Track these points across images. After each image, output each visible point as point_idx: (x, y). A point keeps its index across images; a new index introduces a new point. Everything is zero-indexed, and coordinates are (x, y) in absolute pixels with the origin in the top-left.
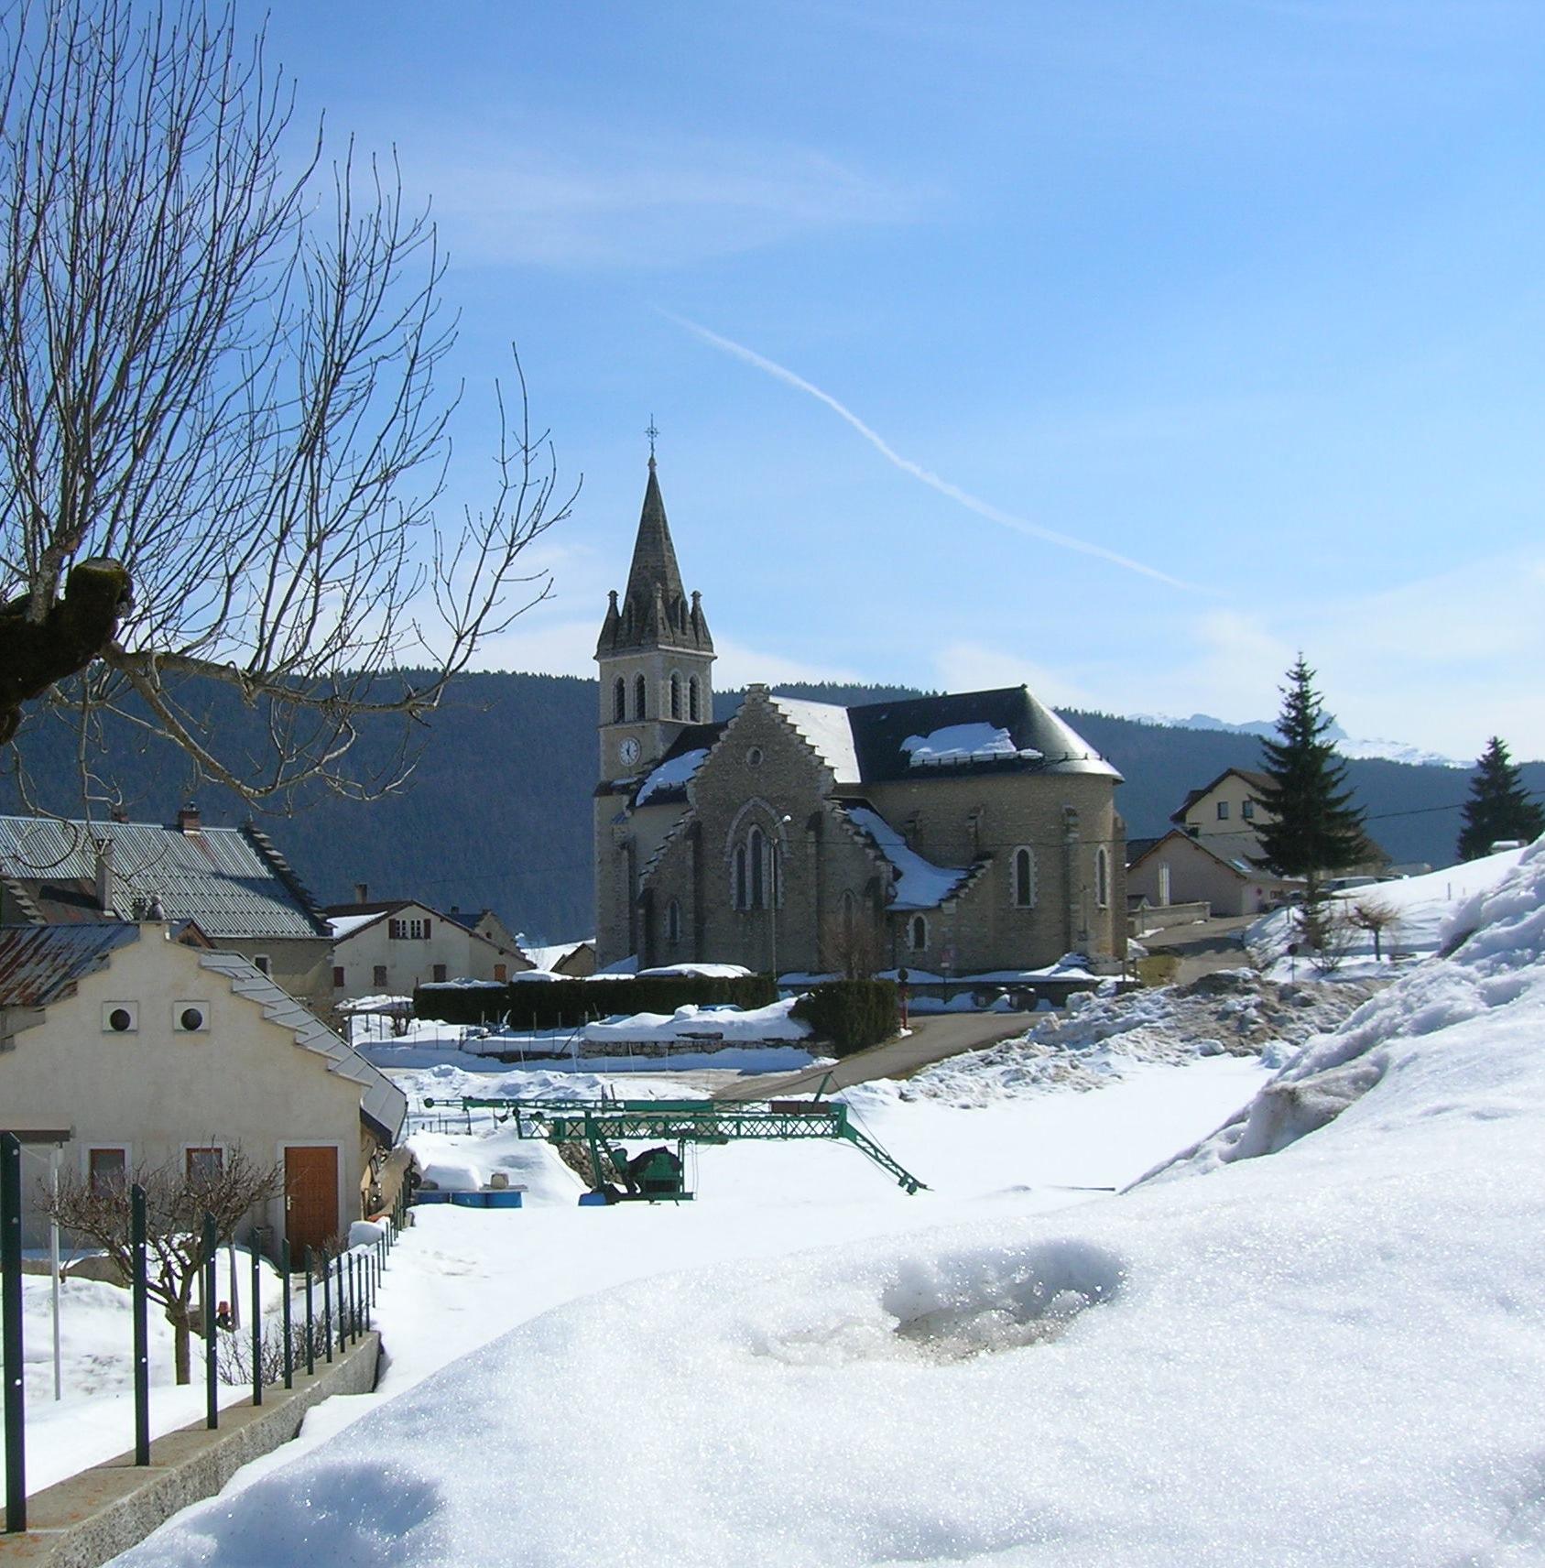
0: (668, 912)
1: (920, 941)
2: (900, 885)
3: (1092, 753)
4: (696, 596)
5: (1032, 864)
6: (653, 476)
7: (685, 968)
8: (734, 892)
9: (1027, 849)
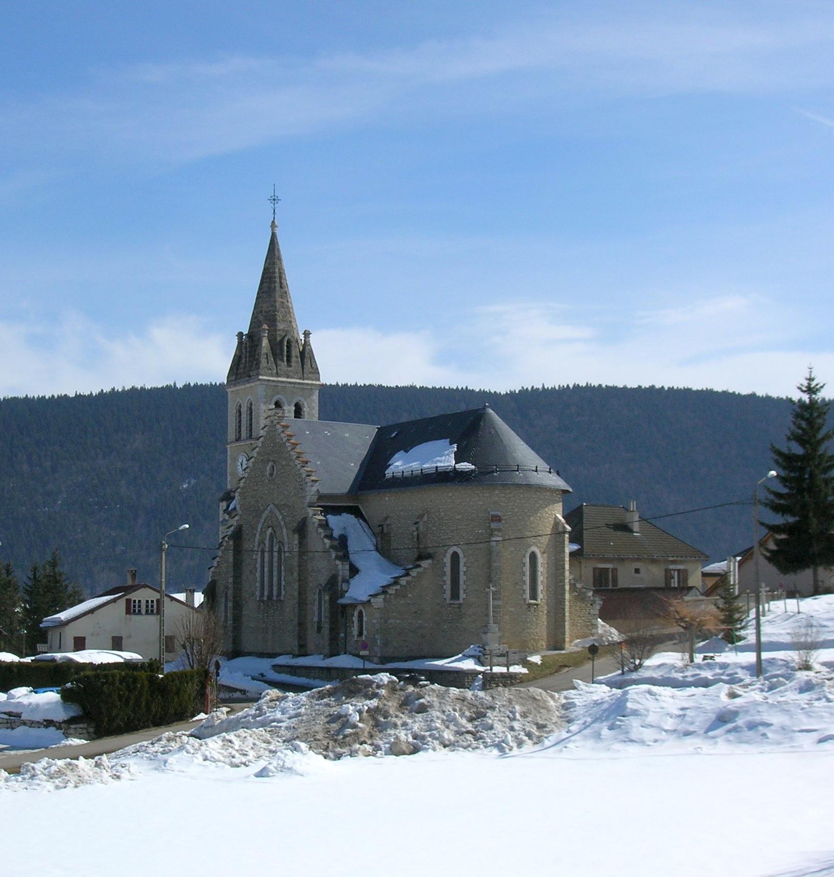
0: (223, 600)
1: (360, 634)
4: (307, 334)
5: (461, 564)
6: (274, 237)
7: (58, 656)
8: (258, 584)
9: (459, 551)
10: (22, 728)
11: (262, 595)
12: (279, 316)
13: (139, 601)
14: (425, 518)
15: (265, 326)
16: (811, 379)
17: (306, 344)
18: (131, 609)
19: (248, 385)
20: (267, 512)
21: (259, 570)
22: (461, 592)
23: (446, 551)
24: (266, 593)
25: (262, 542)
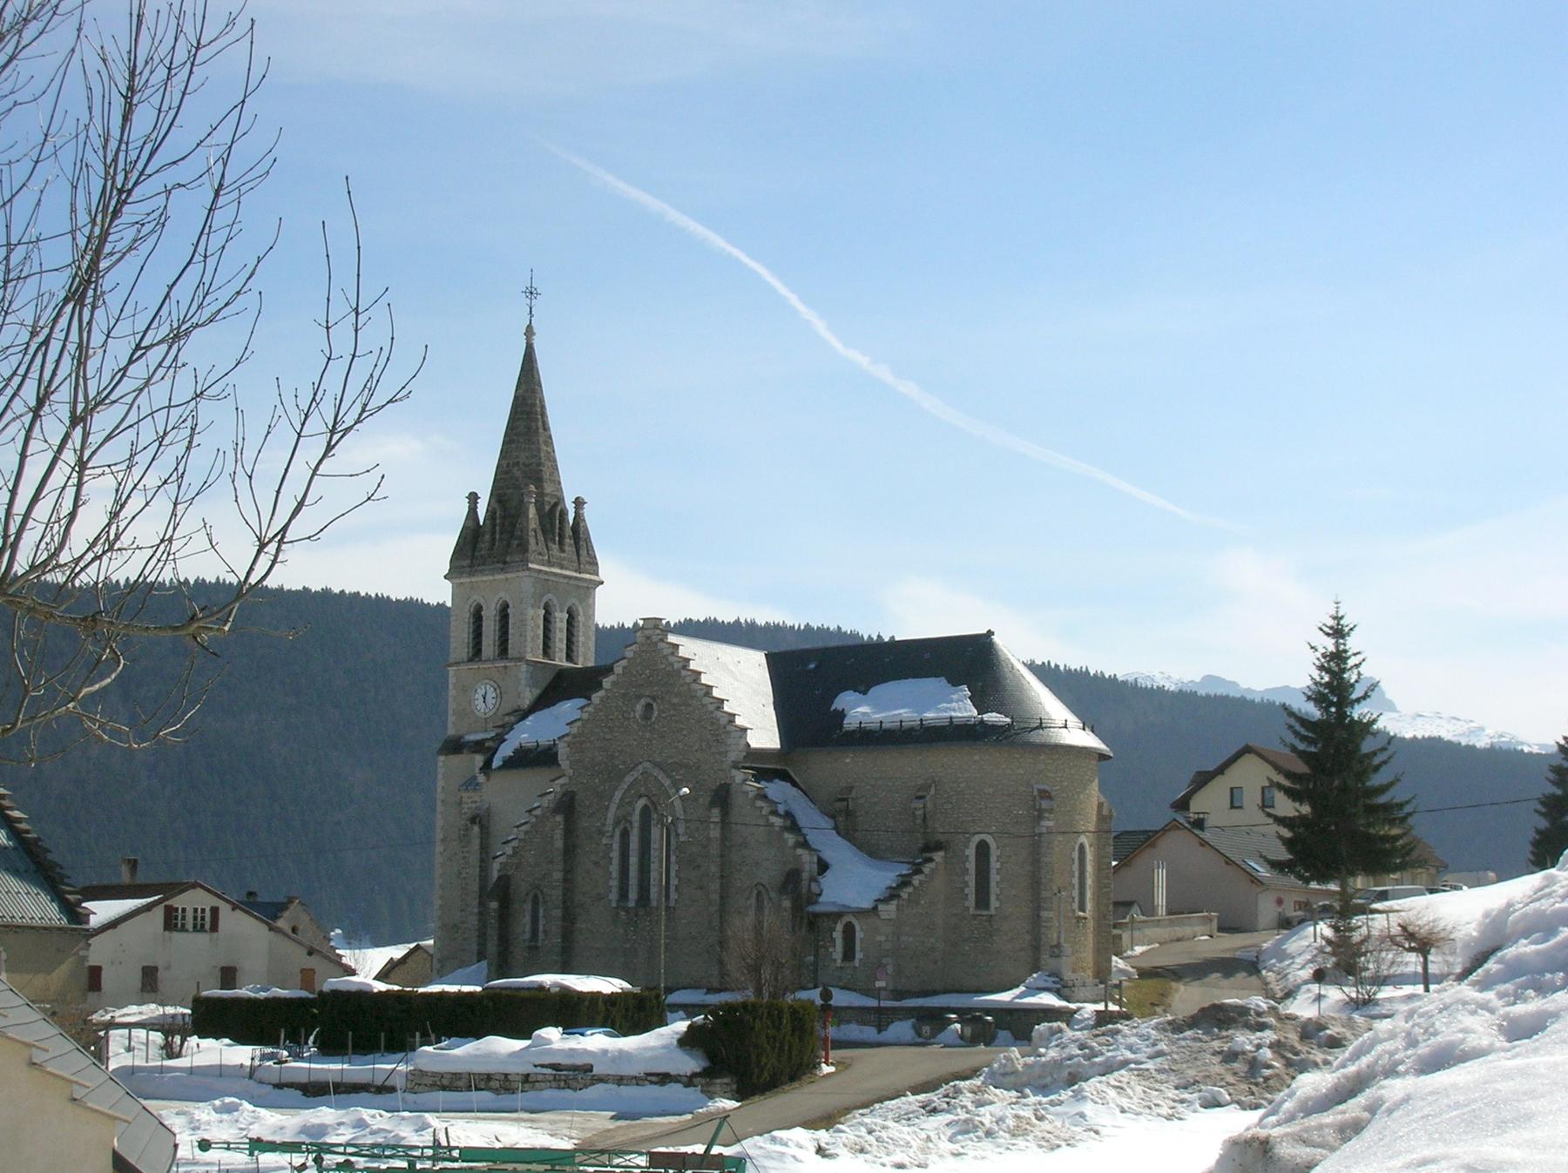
0: (528, 906)
1: (849, 954)
2: (827, 880)
3: (1073, 720)
4: (579, 503)
5: (993, 859)
7: (548, 979)
8: (614, 883)
9: (989, 839)
10: (600, 1086)
11: (623, 895)
12: (546, 476)
13: (184, 910)
14: (932, 792)
15: (532, 488)
16: (1338, 618)
17: (578, 517)
18: (172, 921)
19: (498, 577)
20: (635, 774)
21: (616, 861)
22: (993, 898)
23: (969, 840)
24: (633, 895)
25: (623, 820)
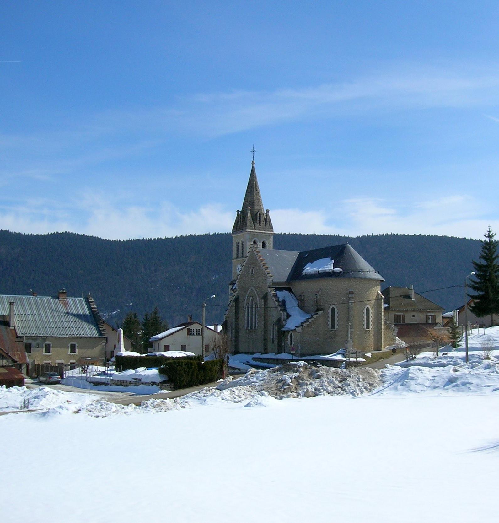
0: (230, 329)
1: (291, 344)
2: (289, 321)
3: (372, 269)
4: (268, 211)
5: (336, 313)
6: (253, 167)
7: (158, 353)
8: (246, 322)
9: (335, 307)
10: (142, 385)
12: (255, 203)
15: (249, 208)
16: (490, 232)
17: (268, 215)
18: (190, 333)
22: (336, 325)
24: (249, 326)
25: (248, 303)
